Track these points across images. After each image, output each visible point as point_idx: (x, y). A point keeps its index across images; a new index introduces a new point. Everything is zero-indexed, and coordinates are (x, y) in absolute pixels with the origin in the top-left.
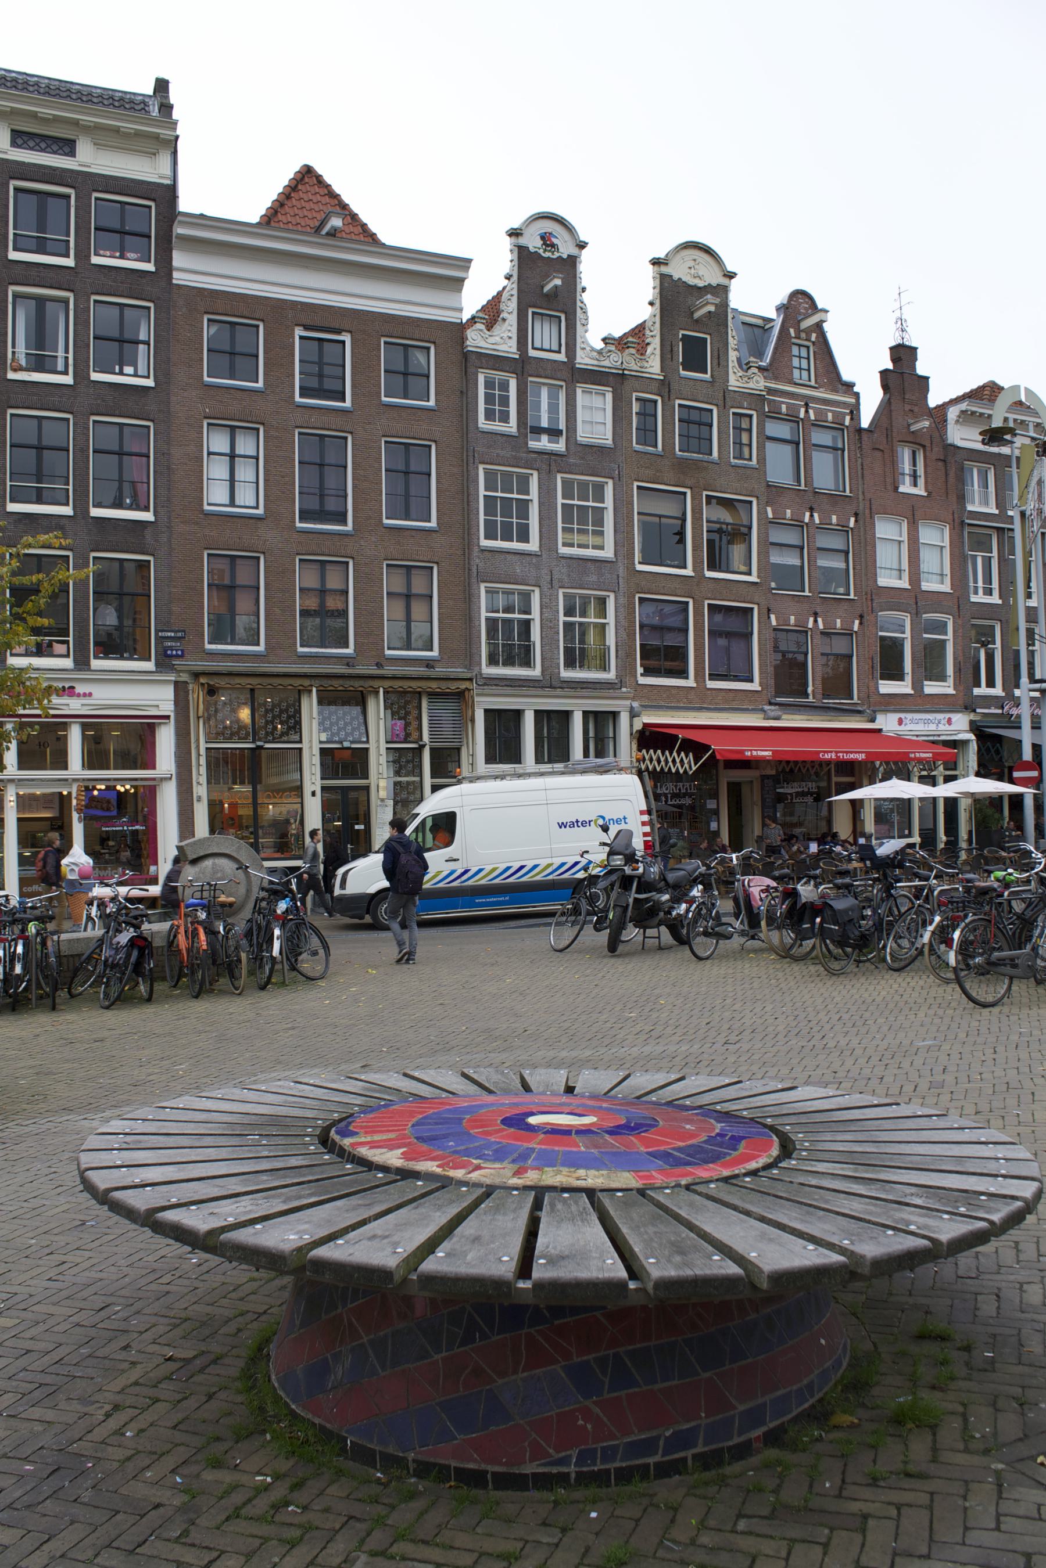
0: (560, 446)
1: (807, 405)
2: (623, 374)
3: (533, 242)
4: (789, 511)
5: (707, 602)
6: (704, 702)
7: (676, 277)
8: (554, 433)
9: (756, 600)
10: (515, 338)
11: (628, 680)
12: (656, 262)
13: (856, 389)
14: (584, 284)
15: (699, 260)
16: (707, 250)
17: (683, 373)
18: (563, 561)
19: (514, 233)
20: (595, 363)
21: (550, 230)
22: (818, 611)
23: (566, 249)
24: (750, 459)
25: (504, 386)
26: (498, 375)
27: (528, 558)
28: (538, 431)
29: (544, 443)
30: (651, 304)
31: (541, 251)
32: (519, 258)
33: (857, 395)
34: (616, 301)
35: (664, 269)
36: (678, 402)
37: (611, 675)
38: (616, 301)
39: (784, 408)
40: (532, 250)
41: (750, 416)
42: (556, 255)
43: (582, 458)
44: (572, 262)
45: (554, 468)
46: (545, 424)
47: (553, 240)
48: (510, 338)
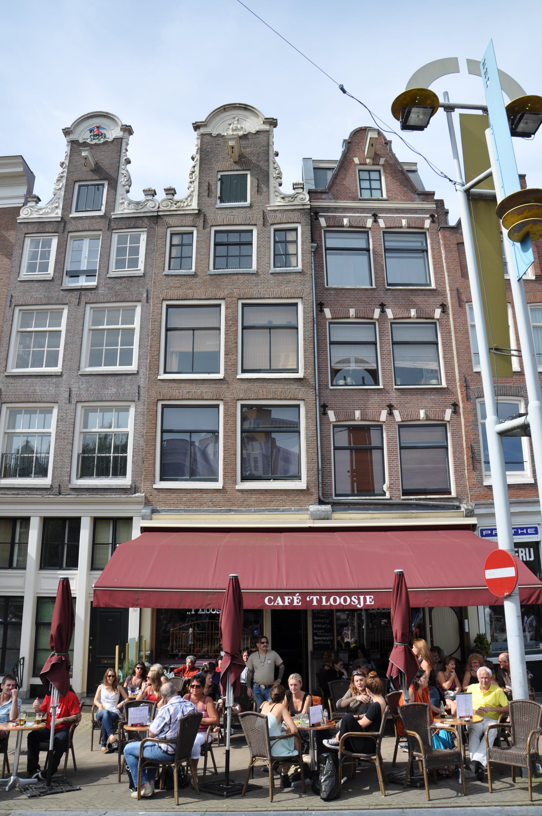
0: (93, 283)
1: (375, 216)
2: (158, 216)
3: (83, 135)
4: (352, 312)
5: (239, 403)
6: (233, 504)
7: (215, 133)
8: (90, 274)
9: (300, 397)
10: (61, 207)
11: (142, 486)
12: (197, 127)
13: (436, 198)
14: (129, 155)
15: (240, 117)
16: (245, 108)
17: (219, 205)
18: (83, 379)
19: (67, 132)
20: (135, 211)
21: (98, 125)
22: (393, 403)
23: (113, 133)
24: (297, 266)
25: (48, 244)
26: (42, 237)
27: (49, 379)
28: (75, 275)
29: (82, 282)
30: (193, 158)
31: (88, 141)
32: (71, 150)
33: (440, 203)
34: (162, 165)
35: (202, 130)
36: (214, 229)
37: (126, 481)
38: (162, 165)
39: (346, 221)
40: (81, 141)
41: (296, 230)
42: (102, 141)
43: (112, 288)
44: (118, 142)
45: (83, 300)
46: (84, 267)
47: (101, 131)
48: (57, 207)
